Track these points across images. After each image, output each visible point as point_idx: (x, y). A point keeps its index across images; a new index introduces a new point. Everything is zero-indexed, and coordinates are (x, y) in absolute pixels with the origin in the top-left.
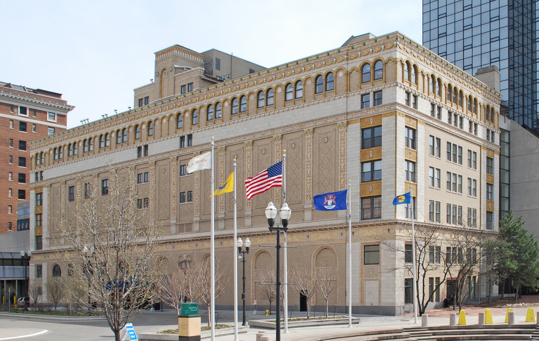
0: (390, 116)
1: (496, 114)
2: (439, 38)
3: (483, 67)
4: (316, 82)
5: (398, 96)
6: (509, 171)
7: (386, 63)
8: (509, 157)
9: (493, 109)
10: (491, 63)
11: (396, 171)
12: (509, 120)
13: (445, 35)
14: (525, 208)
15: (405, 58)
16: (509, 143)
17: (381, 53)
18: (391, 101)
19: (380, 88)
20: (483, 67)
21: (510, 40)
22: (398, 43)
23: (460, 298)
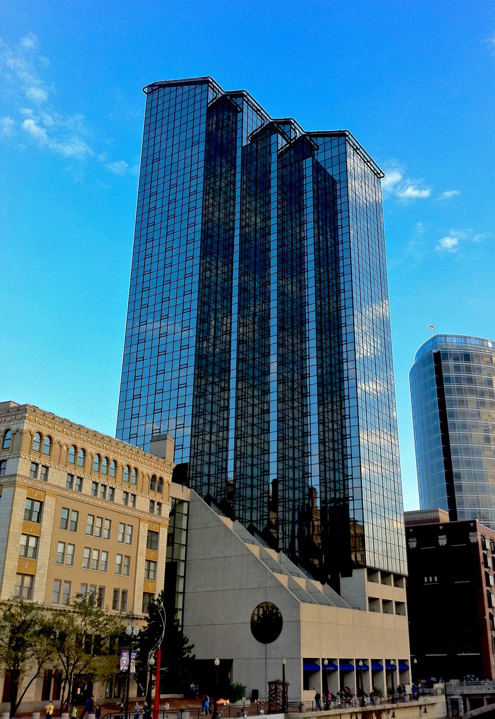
0: (9, 487)
1: (167, 484)
2: (133, 399)
3: (161, 433)
4: (5, 436)
5: (19, 467)
6: (186, 546)
7: (14, 434)
8: (187, 530)
9: (161, 479)
10: (153, 433)
11: (7, 546)
12: (189, 489)
13: (139, 396)
14: (199, 589)
15: (34, 430)
16: (188, 515)
17: (11, 423)
18: (13, 473)
19: (5, 458)
20: (161, 433)
21: (279, 394)
22: (27, 415)
23: (63, 696)
